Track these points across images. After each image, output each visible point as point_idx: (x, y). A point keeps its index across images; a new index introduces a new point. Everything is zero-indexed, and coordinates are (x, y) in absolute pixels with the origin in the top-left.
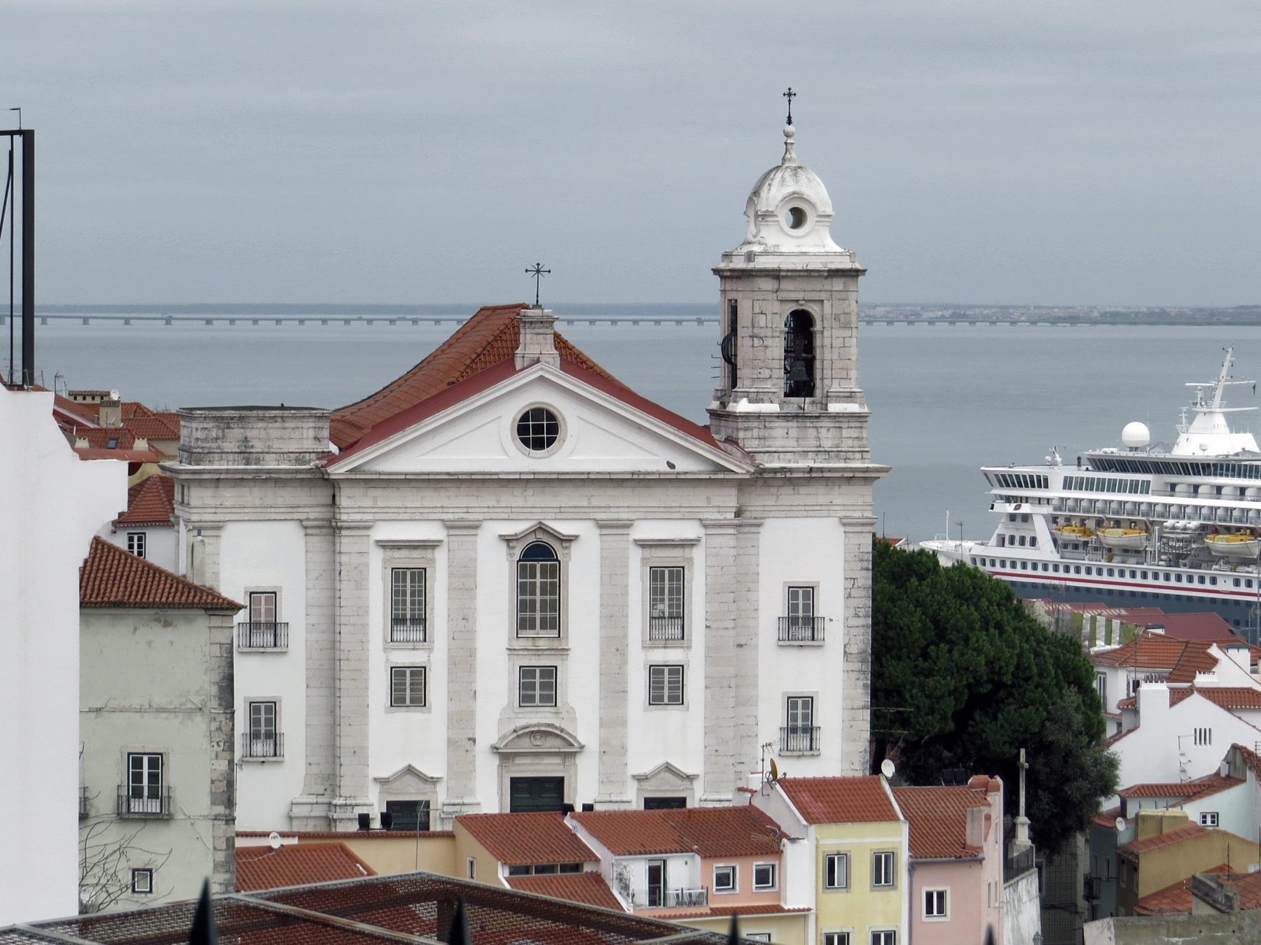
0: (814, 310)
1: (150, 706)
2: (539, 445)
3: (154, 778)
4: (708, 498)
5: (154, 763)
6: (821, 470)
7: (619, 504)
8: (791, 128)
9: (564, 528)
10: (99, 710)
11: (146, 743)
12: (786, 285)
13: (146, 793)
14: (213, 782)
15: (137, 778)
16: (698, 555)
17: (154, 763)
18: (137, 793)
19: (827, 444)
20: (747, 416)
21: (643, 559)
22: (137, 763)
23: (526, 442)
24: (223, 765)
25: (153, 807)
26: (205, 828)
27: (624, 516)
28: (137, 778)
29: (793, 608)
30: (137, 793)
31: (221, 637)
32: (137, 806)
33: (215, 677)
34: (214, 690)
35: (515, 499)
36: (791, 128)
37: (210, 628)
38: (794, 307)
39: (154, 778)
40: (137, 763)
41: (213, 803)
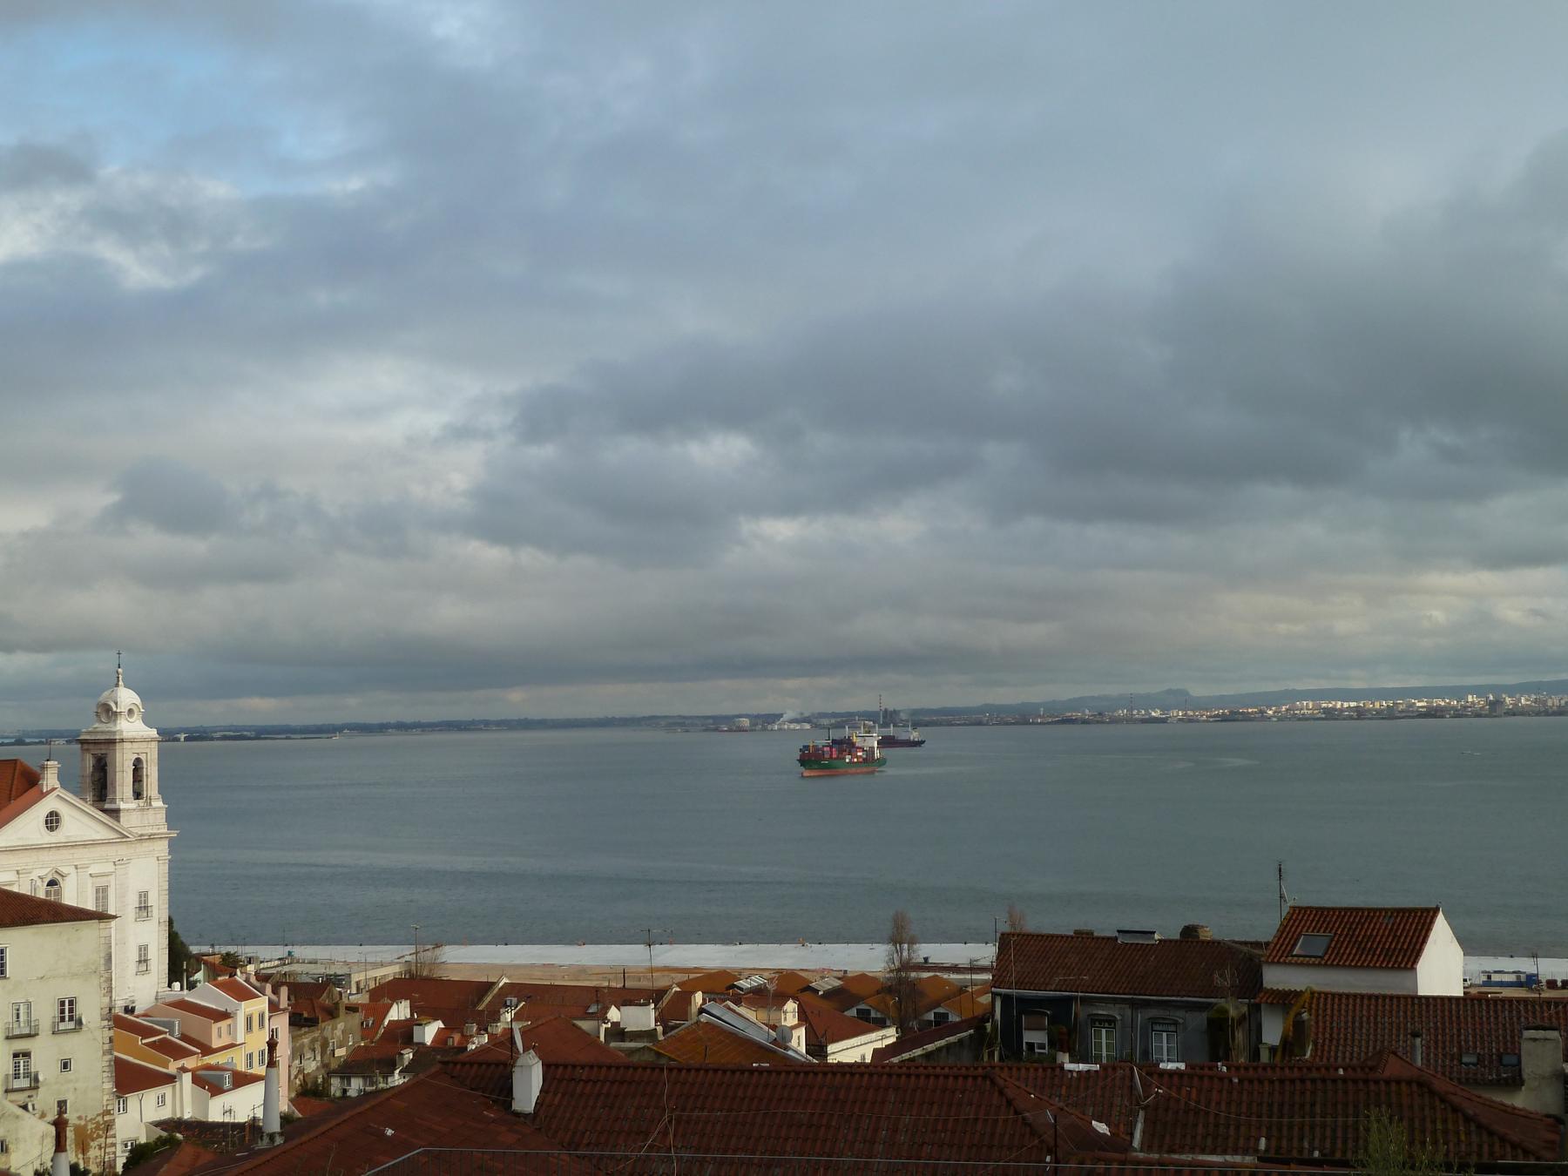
0: (143, 757)
1: (69, 973)
2: (51, 829)
3: (71, 1011)
4: (117, 851)
5: (71, 1003)
6: (155, 834)
7: (82, 855)
8: (120, 670)
9: (64, 870)
10: (42, 978)
11: (66, 994)
12: (135, 745)
13: (67, 1019)
14: (102, 1009)
15: (62, 1012)
16: (112, 878)
17: (71, 1003)
18: (63, 1019)
19: (151, 821)
20: (124, 810)
21: (93, 883)
22: (62, 1004)
23: (47, 827)
24: (107, 1000)
25: (71, 1025)
26: (98, 1034)
27: (86, 862)
28: (62, 1012)
29: (140, 903)
30: (63, 1019)
31: (103, 933)
32: (62, 1026)
33: (102, 955)
34: (102, 961)
35: (45, 856)
36: (120, 670)
37: (99, 929)
38: (136, 756)
39: (71, 1011)
40: (62, 1004)
41: (102, 1020)
